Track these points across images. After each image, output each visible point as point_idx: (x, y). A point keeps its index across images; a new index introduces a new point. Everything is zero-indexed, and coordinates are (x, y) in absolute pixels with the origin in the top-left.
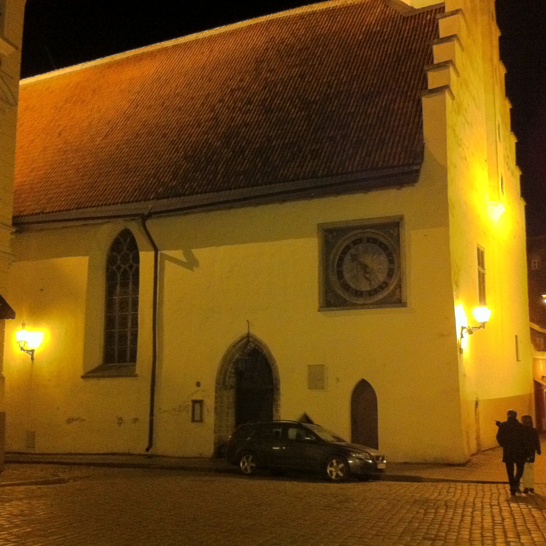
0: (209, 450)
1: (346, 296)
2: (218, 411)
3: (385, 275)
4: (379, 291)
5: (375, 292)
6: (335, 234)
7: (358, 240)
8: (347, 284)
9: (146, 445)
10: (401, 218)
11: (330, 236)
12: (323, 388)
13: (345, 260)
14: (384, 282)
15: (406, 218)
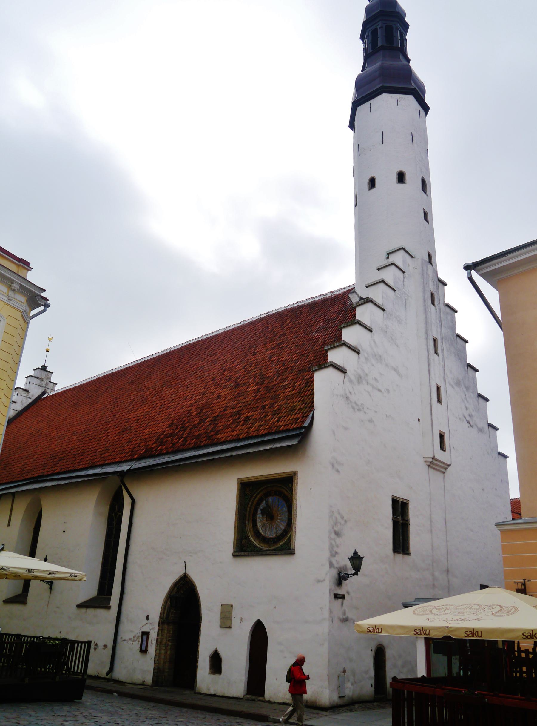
0: (149, 679)
1: (256, 543)
2: (159, 643)
3: (285, 524)
8: (259, 532)
9: (107, 668)
12: (230, 627)
15: (299, 475)
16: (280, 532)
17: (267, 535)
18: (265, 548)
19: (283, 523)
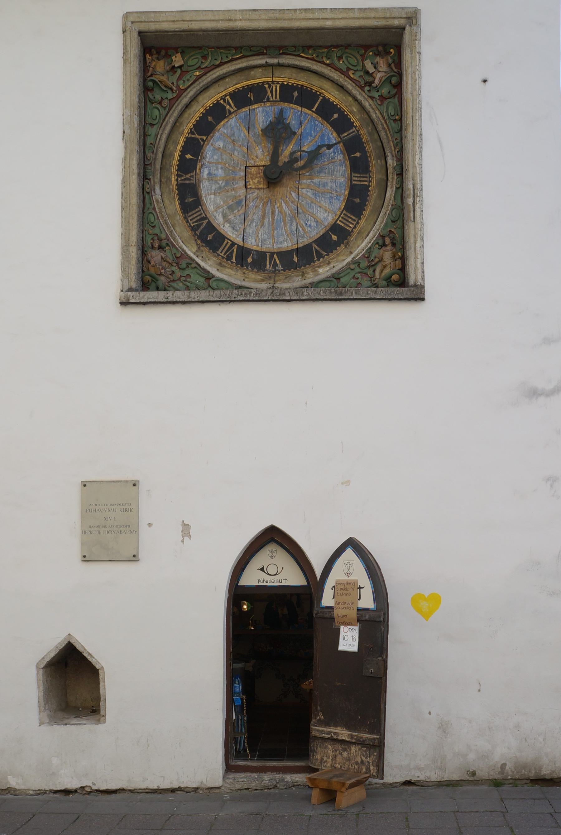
3: (339, 205)
4: (320, 256)
6: (178, 60)
7: (251, 88)
8: (211, 228)
10: (412, 17)
11: (160, 66)
13: (209, 153)
14: (335, 228)
15: (426, 24)
16: (315, 233)
17: (251, 243)
18: (253, 280)
19: (324, 203)
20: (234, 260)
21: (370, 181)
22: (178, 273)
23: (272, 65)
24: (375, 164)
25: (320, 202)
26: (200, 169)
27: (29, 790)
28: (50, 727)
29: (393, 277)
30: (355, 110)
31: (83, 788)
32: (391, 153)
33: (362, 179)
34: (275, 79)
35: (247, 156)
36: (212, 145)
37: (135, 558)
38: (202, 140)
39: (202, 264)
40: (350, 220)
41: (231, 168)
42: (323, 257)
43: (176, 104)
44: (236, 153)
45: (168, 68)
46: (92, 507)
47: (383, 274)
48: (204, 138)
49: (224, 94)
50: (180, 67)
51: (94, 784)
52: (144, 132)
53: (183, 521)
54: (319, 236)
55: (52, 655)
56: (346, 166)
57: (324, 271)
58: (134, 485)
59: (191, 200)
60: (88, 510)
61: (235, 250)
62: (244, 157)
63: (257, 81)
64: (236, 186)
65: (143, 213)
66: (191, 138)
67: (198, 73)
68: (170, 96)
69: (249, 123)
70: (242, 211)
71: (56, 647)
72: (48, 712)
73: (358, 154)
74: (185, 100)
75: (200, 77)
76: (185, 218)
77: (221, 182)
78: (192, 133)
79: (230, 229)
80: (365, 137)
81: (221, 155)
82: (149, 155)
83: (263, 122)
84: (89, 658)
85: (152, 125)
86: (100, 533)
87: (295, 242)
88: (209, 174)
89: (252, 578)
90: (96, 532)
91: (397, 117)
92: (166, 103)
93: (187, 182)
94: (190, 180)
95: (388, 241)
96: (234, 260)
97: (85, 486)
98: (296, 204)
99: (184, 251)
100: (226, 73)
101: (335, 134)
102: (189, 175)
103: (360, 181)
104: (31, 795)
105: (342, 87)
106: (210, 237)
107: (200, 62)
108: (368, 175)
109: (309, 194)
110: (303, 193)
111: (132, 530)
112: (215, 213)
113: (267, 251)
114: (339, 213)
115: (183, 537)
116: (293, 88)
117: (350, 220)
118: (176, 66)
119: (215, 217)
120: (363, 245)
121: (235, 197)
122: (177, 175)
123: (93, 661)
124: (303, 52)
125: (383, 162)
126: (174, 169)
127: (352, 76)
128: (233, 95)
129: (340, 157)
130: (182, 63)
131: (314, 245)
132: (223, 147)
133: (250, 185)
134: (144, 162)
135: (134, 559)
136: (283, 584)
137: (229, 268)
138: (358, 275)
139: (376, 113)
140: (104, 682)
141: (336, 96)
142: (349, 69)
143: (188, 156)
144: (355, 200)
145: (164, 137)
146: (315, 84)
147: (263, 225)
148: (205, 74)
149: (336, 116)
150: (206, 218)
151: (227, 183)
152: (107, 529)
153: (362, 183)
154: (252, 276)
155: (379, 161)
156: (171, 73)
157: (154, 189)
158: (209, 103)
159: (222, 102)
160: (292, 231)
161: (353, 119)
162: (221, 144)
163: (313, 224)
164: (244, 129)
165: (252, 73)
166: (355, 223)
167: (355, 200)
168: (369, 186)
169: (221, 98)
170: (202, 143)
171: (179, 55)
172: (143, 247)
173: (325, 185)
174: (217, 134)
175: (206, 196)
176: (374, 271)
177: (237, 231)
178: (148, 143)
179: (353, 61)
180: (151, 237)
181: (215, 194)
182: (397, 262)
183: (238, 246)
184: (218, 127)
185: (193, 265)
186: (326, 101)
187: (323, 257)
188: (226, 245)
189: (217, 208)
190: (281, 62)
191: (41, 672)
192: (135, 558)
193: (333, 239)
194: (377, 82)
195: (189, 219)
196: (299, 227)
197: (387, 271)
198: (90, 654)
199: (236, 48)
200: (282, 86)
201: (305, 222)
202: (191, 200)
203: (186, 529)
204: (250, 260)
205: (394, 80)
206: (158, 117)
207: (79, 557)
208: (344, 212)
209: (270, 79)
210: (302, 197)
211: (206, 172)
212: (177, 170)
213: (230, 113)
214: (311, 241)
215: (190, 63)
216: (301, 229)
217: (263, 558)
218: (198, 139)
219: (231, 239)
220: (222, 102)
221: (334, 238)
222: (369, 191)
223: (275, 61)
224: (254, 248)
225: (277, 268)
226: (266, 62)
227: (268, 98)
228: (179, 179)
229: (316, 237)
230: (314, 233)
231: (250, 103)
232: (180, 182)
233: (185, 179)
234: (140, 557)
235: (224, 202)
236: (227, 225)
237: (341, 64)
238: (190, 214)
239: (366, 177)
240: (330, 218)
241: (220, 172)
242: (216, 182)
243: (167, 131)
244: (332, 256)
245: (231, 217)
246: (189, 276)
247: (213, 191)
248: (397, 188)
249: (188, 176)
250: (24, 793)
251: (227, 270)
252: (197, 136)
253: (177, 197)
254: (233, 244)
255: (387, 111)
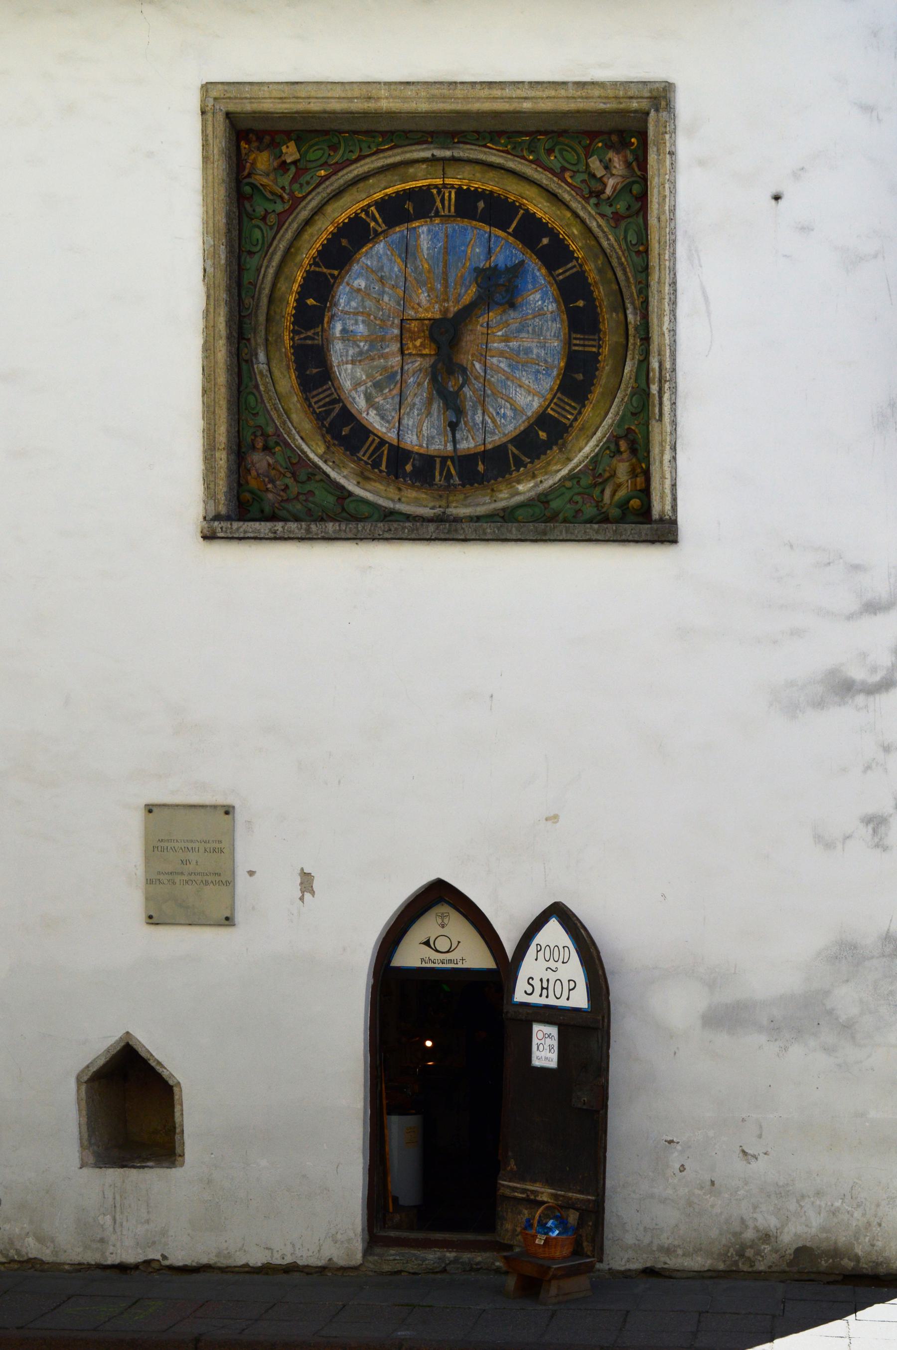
1: (344, 477)
3: (548, 384)
4: (519, 464)
5: (496, 464)
7: (409, 194)
8: (347, 416)
11: (263, 161)
13: (343, 299)
14: (542, 420)
17: (411, 441)
18: (414, 502)
19: (526, 380)
20: (383, 467)
21: (600, 347)
22: (294, 489)
23: (443, 160)
24: (608, 320)
25: (519, 379)
26: (329, 322)
27: (64, 1264)
28: (97, 1170)
29: (627, 506)
30: (576, 232)
31: (148, 1263)
32: (633, 303)
33: (586, 343)
34: (447, 181)
35: (405, 301)
36: (348, 284)
37: (229, 921)
38: (332, 276)
39: (333, 474)
40: (568, 408)
41: (377, 322)
42: (525, 466)
43: (290, 220)
44: (386, 298)
45: (275, 164)
46: (162, 844)
47: (617, 497)
48: (336, 273)
49: (366, 203)
50: (295, 163)
51: (165, 1257)
52: (239, 265)
53: (302, 869)
54: (518, 432)
55: (101, 1062)
56: (562, 321)
57: (526, 489)
58: (227, 813)
59: (315, 371)
60: (155, 848)
61: (386, 452)
62: (399, 304)
63: (419, 184)
64: (387, 350)
65: (239, 392)
66: (314, 272)
67: (323, 173)
68: (279, 207)
69: (407, 251)
70: (396, 391)
71: (108, 1050)
72: (95, 1148)
73: (581, 303)
74: (304, 214)
75: (327, 177)
76: (307, 399)
77: (362, 344)
78: (316, 264)
79: (378, 418)
80: (593, 276)
81: (363, 301)
82: (247, 301)
83: (428, 249)
84: (157, 1068)
85: (251, 253)
86: (174, 883)
87: (480, 441)
88: (344, 330)
89: (411, 955)
90: (169, 881)
91: (641, 248)
92: (272, 219)
93: (309, 342)
94: (313, 339)
95: (623, 445)
96: (383, 467)
97: (150, 811)
98: (482, 380)
99: (304, 453)
100: (369, 172)
101: (544, 271)
102: (312, 331)
103: (584, 346)
104: (68, 1271)
105: (554, 197)
106: (345, 431)
107: (326, 155)
108: (596, 337)
109: (502, 365)
110: (492, 364)
111: (224, 880)
112: (353, 393)
113: (435, 454)
114: (549, 396)
115: (303, 892)
116: (478, 195)
117: (568, 408)
118: (288, 161)
119: (354, 399)
120: (587, 449)
121: (385, 368)
122: (293, 331)
123: (165, 1074)
124: (491, 141)
125: (621, 316)
126: (287, 322)
127: (569, 180)
128: (380, 205)
129: (552, 307)
130: (297, 156)
131: (510, 446)
132: (365, 287)
133: (408, 349)
134: (240, 312)
135: (227, 923)
136: (460, 966)
137: (375, 481)
138: (577, 498)
139: (608, 239)
140: (182, 1105)
141: (546, 210)
142: (564, 169)
143: (311, 301)
144: (576, 376)
145: (271, 271)
146: (513, 190)
147: (429, 414)
148: (335, 173)
149: (545, 241)
150: (339, 400)
151: (372, 347)
152: (185, 878)
153: (587, 349)
154: (411, 494)
155: (614, 315)
156: (281, 171)
157: (256, 354)
158: (343, 218)
159: (363, 215)
160: (475, 424)
161: (573, 247)
162: (361, 283)
163: (509, 413)
164: (399, 260)
165: (411, 170)
166: (575, 412)
167: (576, 376)
168: (599, 354)
169: (363, 209)
170: (332, 281)
171: (292, 144)
172: (239, 445)
173: (528, 351)
174: (356, 267)
175: (338, 366)
176: (602, 492)
177: (388, 422)
178: (245, 281)
179: (571, 157)
180: (252, 430)
181: (353, 362)
182: (638, 479)
183: (391, 445)
184: (358, 256)
185: (318, 477)
186: (529, 217)
187: (525, 466)
188: (370, 445)
189: (357, 385)
190: (456, 154)
191: (83, 1087)
192: (229, 921)
193: (542, 436)
194: (609, 191)
195: (313, 401)
196: (487, 418)
197: (622, 493)
198: (159, 1063)
199: (383, 134)
200: (459, 191)
201: (496, 410)
202: (315, 371)
203: (307, 882)
204: (409, 468)
205: (636, 189)
206: (260, 242)
207: (141, 916)
208: (559, 395)
209: (439, 181)
210: (492, 369)
211: (338, 327)
212: (293, 323)
213: (377, 234)
214: (504, 440)
215: (311, 156)
216: (489, 421)
217: (427, 927)
218: (324, 274)
219: (380, 434)
220: (363, 215)
221: (543, 435)
222: (599, 362)
223: (448, 153)
224: (416, 449)
225: (452, 481)
226: (433, 155)
227: (437, 212)
228: (297, 338)
229: (514, 434)
230: (510, 428)
231: (409, 220)
232: (297, 342)
233: (305, 338)
234: (239, 917)
235: (367, 377)
236: (373, 413)
237: (553, 160)
238: (315, 393)
239: (594, 340)
240: (536, 405)
241: (361, 328)
242: (355, 344)
243: (275, 263)
244: (538, 464)
245: (379, 400)
246: (311, 493)
247: (350, 358)
248: (640, 362)
249: (310, 333)
250: (55, 1267)
251: (373, 484)
252: (325, 270)
253: (293, 366)
254: (383, 442)
255: (625, 238)
